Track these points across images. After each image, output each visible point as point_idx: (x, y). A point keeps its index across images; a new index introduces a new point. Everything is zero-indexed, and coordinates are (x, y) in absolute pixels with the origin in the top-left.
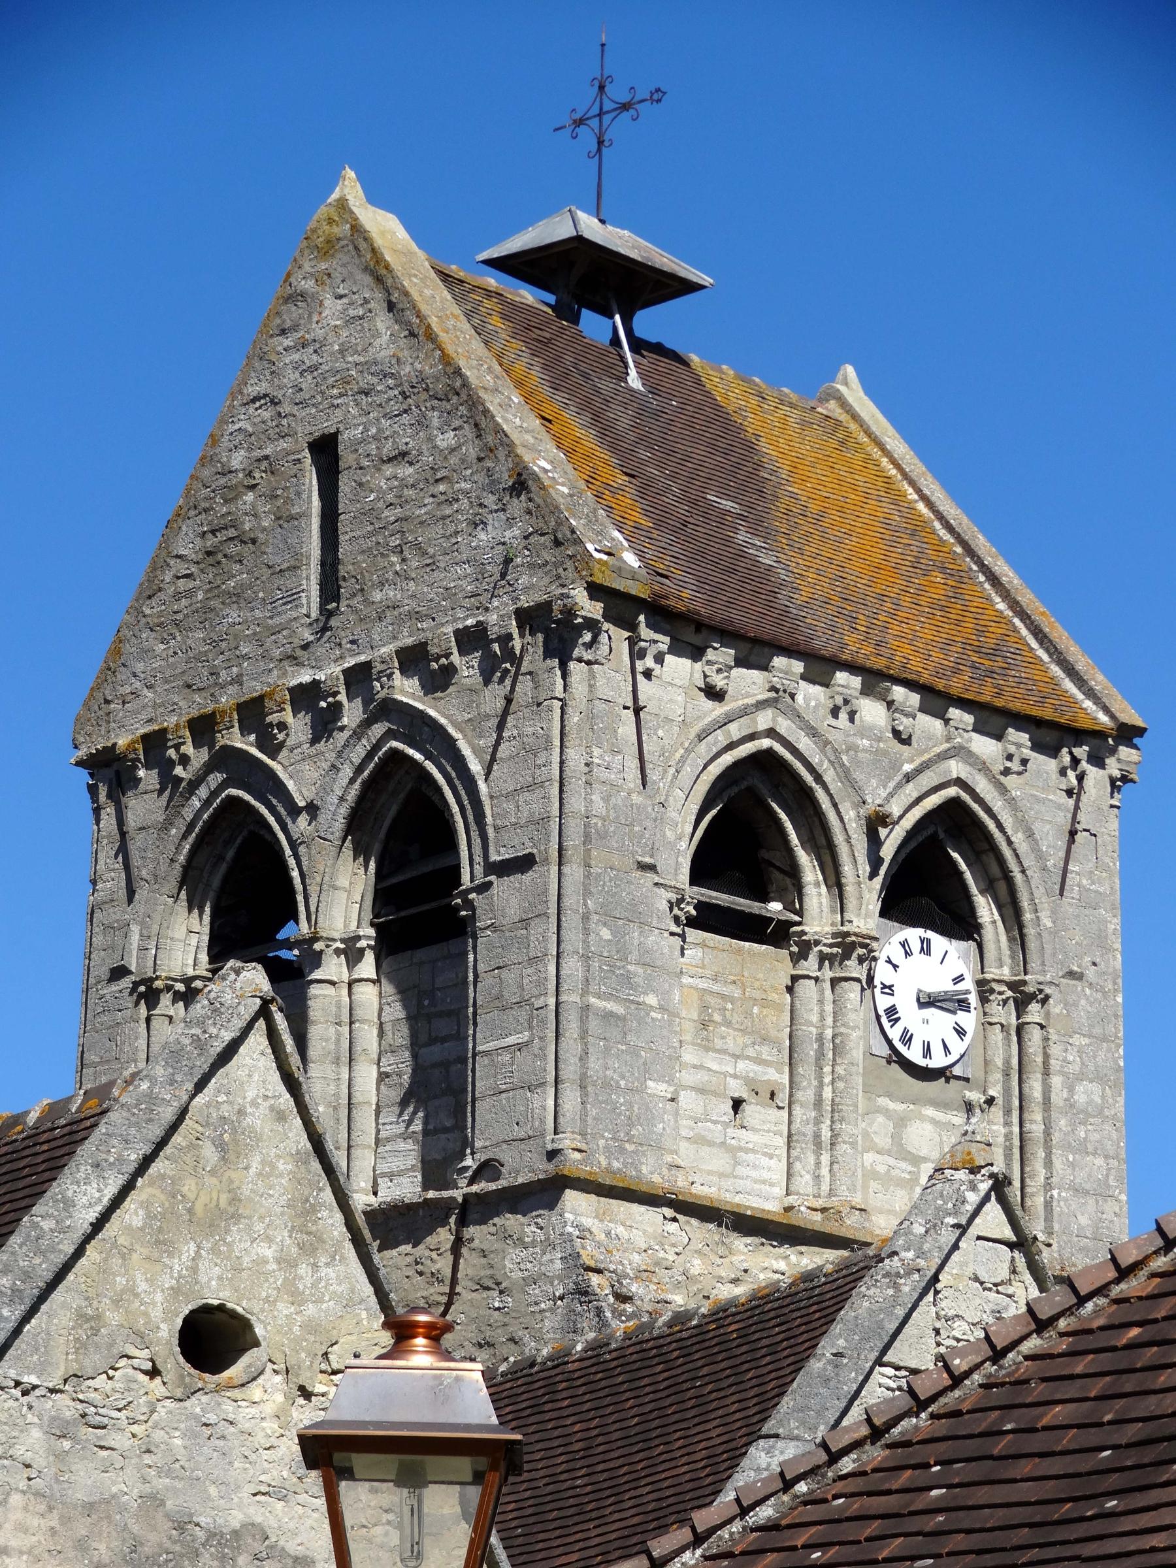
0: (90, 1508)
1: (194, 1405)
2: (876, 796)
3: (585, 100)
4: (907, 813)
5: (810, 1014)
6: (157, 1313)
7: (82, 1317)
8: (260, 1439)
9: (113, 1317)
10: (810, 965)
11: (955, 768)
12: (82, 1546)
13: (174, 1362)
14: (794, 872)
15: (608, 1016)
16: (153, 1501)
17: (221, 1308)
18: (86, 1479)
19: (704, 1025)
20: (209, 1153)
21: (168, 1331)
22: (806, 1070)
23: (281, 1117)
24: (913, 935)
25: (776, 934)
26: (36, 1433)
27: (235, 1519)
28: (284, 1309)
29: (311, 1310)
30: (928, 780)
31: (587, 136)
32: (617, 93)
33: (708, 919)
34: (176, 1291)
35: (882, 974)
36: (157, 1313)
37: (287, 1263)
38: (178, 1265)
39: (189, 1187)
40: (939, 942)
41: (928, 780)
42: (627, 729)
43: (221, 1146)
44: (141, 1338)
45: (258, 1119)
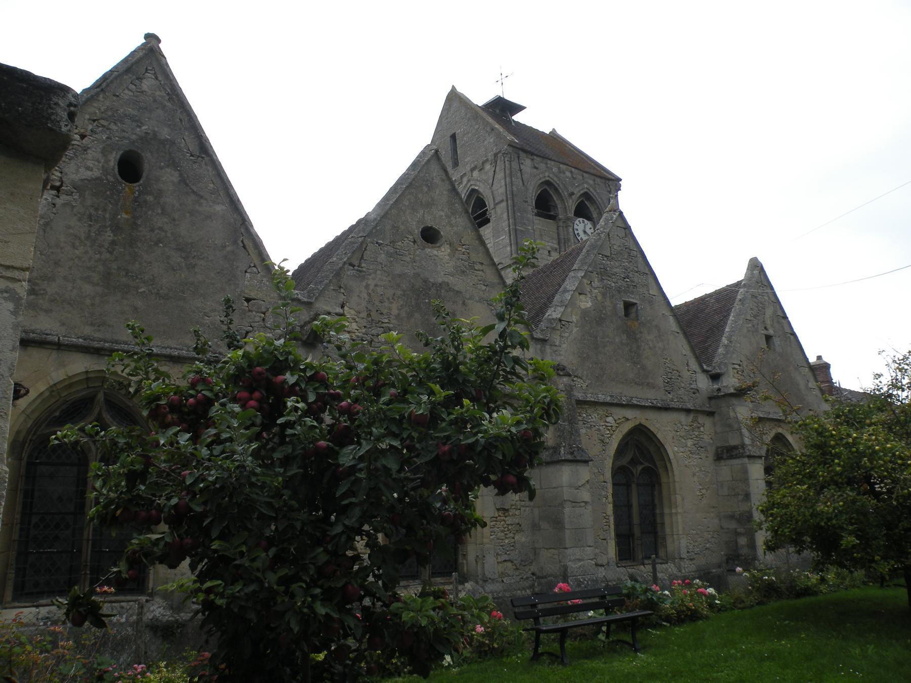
0: (400, 276)
1: (428, 250)
2: (571, 190)
3: (499, 78)
4: (578, 192)
5: (561, 233)
6: (414, 227)
7: (393, 227)
8: (444, 261)
9: (402, 227)
10: (561, 224)
11: (586, 186)
12: (398, 285)
13: (420, 240)
14: (556, 206)
15: (521, 231)
16: (417, 275)
17: (431, 228)
18: (398, 269)
19: (541, 235)
20: (425, 189)
21: (417, 232)
22: (562, 245)
23: (443, 180)
24: (581, 219)
25: (553, 218)
26: (383, 255)
27: (440, 280)
28: (448, 228)
29: (455, 228)
30: (581, 188)
31: (500, 83)
32: (504, 76)
33: (538, 215)
34: (419, 222)
35: (576, 227)
36: (414, 227)
37: (448, 216)
38: (419, 215)
39: (420, 196)
40: (586, 221)
41: (581, 188)
42: (519, 174)
43: (427, 185)
44: (410, 233)
45: (437, 181)
